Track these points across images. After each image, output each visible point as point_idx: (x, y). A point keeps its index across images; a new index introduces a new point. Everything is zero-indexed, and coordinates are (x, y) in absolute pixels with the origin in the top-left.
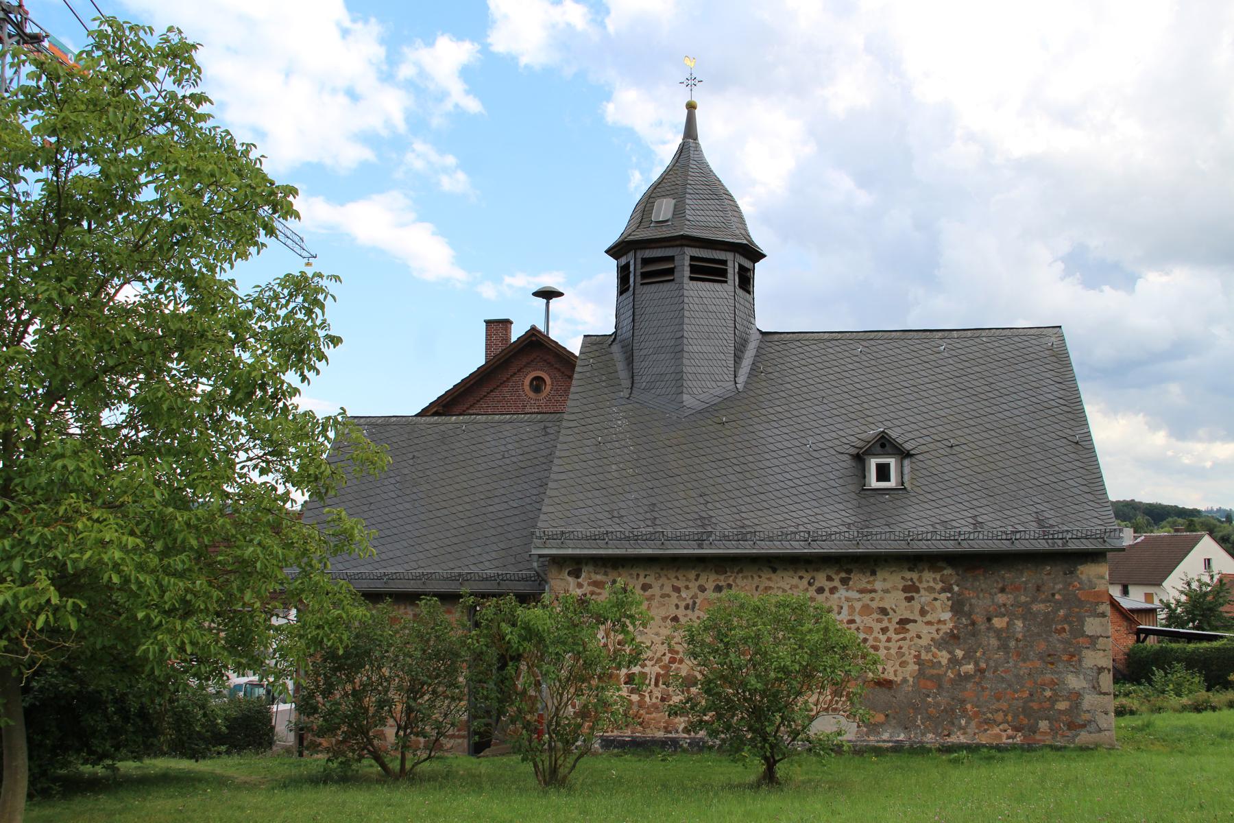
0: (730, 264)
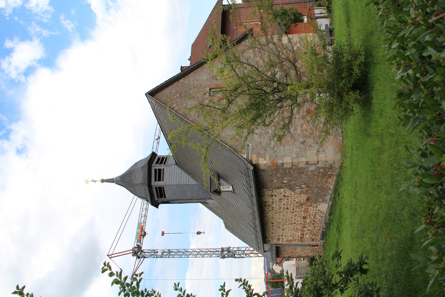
0: (156, 168)
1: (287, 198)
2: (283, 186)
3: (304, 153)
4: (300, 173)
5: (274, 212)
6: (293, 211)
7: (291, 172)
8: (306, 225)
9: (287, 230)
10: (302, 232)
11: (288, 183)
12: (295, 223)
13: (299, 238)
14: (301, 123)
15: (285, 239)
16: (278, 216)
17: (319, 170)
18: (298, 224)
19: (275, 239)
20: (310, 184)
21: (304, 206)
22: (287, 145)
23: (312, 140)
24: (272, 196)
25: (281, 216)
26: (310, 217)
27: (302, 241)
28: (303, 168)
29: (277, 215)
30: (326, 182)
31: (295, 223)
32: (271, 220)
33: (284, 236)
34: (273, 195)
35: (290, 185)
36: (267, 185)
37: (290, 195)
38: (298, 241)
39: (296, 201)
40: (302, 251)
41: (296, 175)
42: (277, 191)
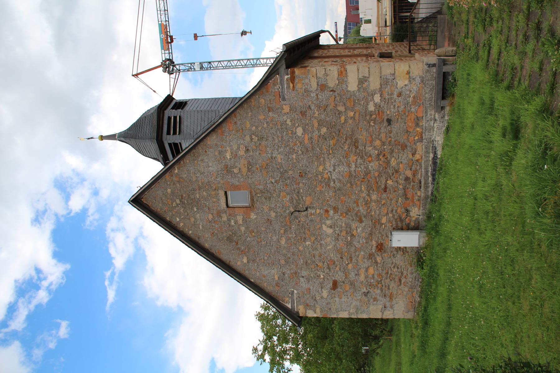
3: (366, 308)
14: (366, 265)
22: (344, 295)
23: (379, 291)
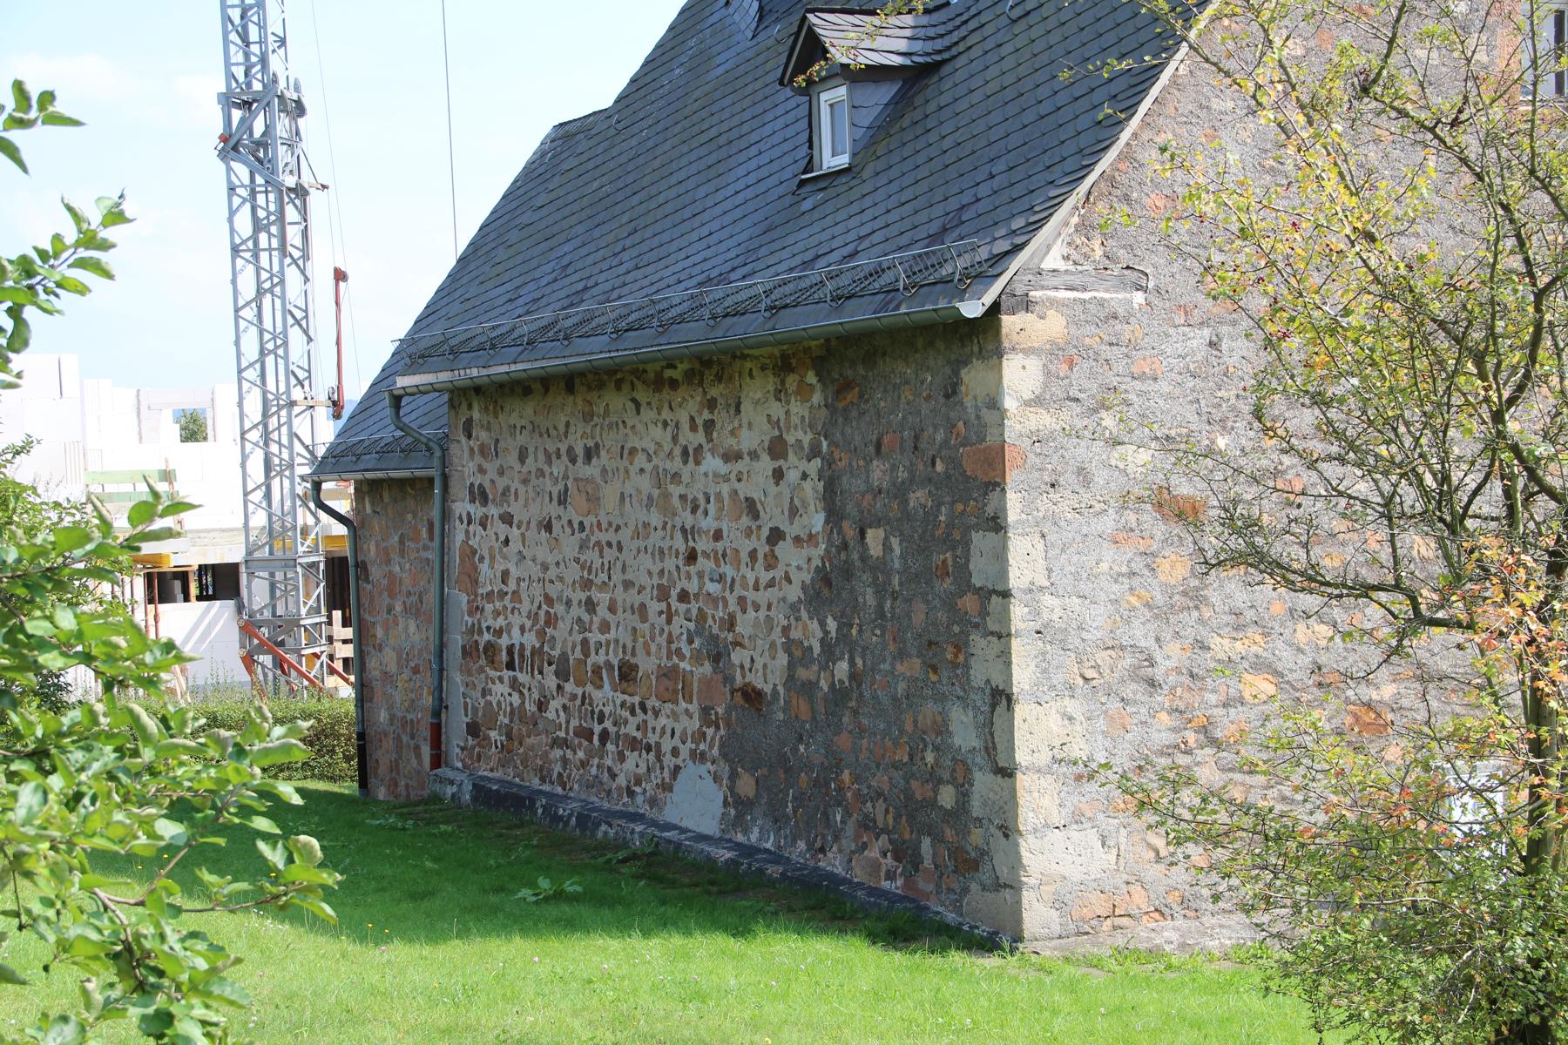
1: (760, 556)
2: (846, 524)
4: (930, 643)
5: (668, 465)
6: (674, 593)
7: (937, 584)
8: (579, 683)
9: (543, 554)
10: (528, 653)
11: (864, 558)
12: (591, 606)
13: (487, 637)
15: (481, 540)
16: (639, 491)
17: (953, 781)
18: (584, 629)
19: (482, 471)
20: (855, 712)
21: (707, 668)
24: (777, 448)
25: (636, 514)
26: (633, 713)
27: (469, 652)
28: (967, 667)
29: (645, 484)
30: (866, 827)
31: (591, 606)
32: (610, 440)
33: (502, 529)
34: (785, 456)
35: (847, 572)
36: (854, 414)
37: (778, 573)
38: (471, 631)
39: (739, 616)
40: (399, 658)
41: (918, 618)
42: (807, 485)
